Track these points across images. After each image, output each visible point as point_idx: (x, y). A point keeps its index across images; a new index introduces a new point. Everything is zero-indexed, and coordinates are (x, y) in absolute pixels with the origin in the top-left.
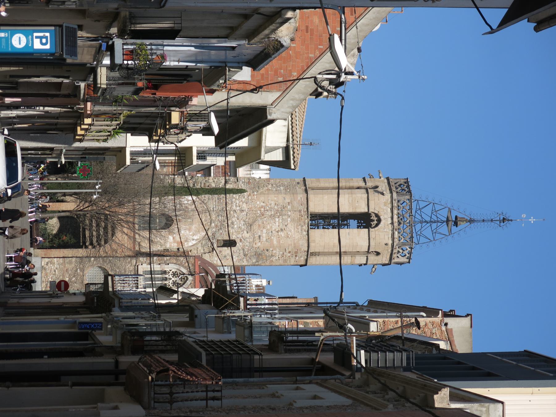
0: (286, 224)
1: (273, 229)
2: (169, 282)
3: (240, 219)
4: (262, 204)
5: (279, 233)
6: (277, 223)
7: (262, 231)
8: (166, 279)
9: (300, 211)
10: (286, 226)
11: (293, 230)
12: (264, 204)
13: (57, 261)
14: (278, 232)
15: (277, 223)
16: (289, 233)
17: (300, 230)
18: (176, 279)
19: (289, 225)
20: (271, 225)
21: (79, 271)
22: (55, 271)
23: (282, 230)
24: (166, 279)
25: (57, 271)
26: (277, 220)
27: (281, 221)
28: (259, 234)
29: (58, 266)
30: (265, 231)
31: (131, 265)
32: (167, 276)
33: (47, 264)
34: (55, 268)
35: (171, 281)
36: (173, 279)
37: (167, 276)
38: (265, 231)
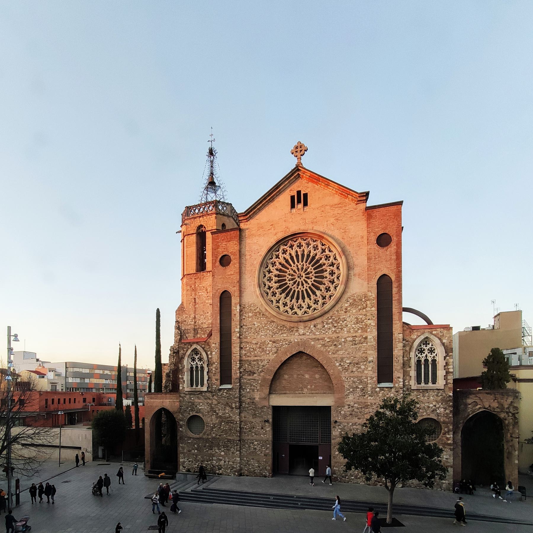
0: (203, 287)
1: (206, 296)
2: (199, 364)
3: (200, 319)
4: (191, 305)
5: (208, 291)
6: (202, 293)
7: (207, 303)
8: (197, 367)
9: (195, 279)
10: (204, 287)
11: (207, 282)
12: (191, 303)
13: (182, 459)
14: (208, 292)
15: (202, 293)
16: (208, 285)
17: (207, 278)
18: (197, 359)
19: (203, 285)
20: (203, 298)
21: (190, 441)
22: (190, 461)
23: (206, 290)
24: (197, 367)
25: (189, 460)
26: (200, 294)
27: (201, 291)
28: (209, 305)
29: (186, 458)
30: (207, 301)
31: (185, 397)
32: (194, 366)
33: (185, 467)
34: (188, 461)
35: (199, 363)
36: (196, 361)
37: (194, 366)
38: (207, 301)
